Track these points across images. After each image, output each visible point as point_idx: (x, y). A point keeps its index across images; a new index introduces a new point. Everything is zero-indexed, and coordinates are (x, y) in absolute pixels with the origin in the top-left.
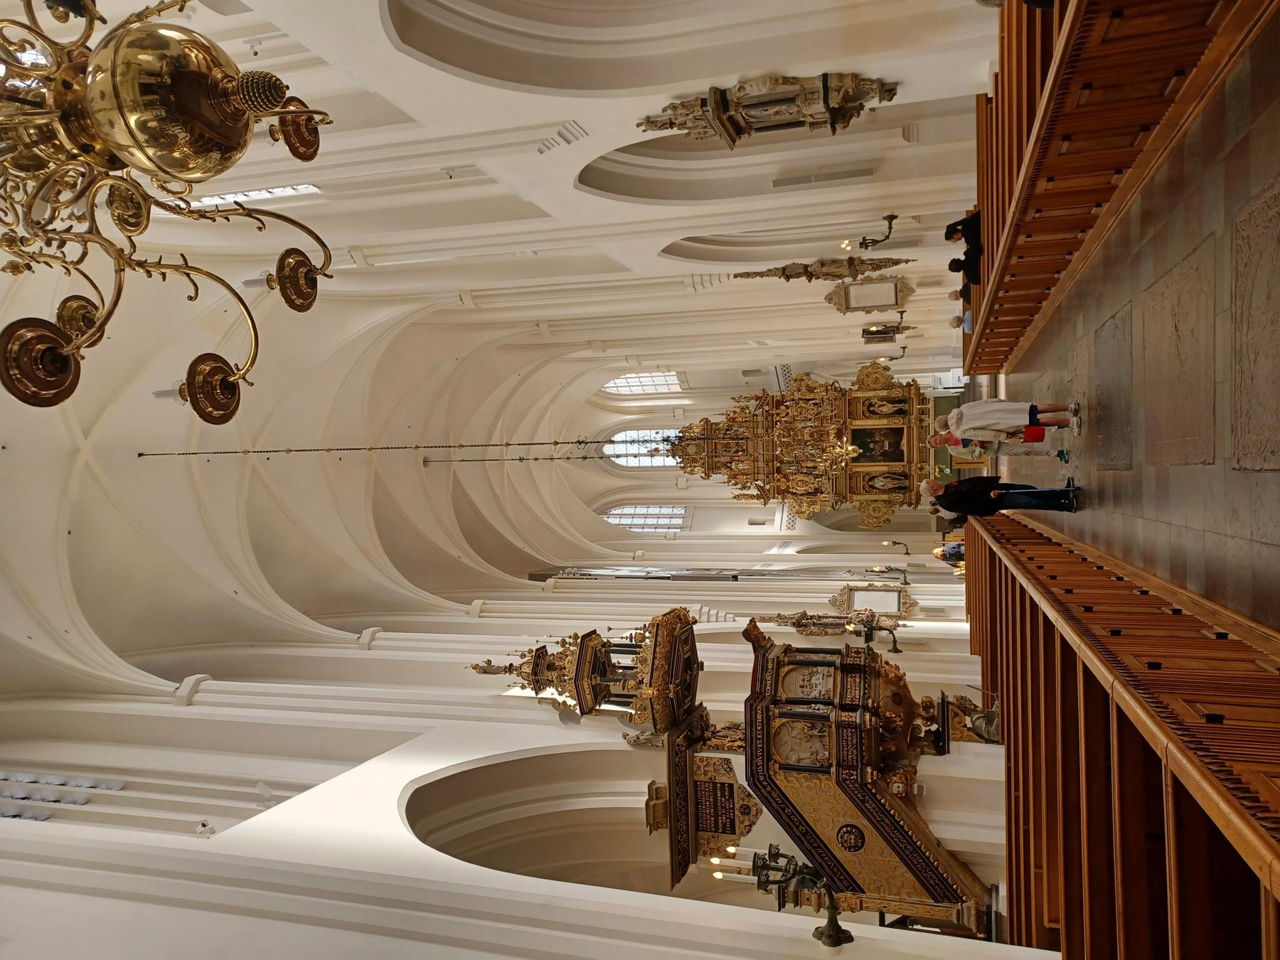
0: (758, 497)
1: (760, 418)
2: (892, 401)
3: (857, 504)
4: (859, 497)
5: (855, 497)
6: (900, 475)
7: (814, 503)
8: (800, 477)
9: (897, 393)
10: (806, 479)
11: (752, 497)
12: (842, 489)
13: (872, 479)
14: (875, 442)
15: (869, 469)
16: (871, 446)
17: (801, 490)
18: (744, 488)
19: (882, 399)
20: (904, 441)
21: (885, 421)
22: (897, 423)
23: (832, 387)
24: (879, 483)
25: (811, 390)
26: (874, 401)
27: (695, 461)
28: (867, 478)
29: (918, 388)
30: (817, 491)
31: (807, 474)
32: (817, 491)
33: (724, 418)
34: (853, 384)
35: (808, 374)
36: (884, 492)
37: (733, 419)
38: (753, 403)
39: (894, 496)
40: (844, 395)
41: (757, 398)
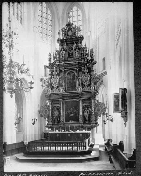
0: (50, 64)
1: (83, 61)
2: (90, 116)
6: (59, 121)
7: (48, 87)
8: (58, 80)
9: (93, 118)
10: (57, 83)
12: (53, 97)
14: (73, 111)
15: (62, 108)
16: (71, 109)
17: (53, 80)
18: (54, 58)
19: (90, 112)
20: (73, 122)
21: (81, 114)
22: (81, 119)
24: (56, 112)
25: (95, 84)
26: (89, 109)
27: (65, 35)
28: (59, 108)
29: (94, 127)
30: (52, 88)
31: (59, 83)
32: (52, 88)
33: (84, 46)
34: (97, 101)
35: (102, 81)
36: (52, 114)
40: (92, 97)
41: (92, 60)
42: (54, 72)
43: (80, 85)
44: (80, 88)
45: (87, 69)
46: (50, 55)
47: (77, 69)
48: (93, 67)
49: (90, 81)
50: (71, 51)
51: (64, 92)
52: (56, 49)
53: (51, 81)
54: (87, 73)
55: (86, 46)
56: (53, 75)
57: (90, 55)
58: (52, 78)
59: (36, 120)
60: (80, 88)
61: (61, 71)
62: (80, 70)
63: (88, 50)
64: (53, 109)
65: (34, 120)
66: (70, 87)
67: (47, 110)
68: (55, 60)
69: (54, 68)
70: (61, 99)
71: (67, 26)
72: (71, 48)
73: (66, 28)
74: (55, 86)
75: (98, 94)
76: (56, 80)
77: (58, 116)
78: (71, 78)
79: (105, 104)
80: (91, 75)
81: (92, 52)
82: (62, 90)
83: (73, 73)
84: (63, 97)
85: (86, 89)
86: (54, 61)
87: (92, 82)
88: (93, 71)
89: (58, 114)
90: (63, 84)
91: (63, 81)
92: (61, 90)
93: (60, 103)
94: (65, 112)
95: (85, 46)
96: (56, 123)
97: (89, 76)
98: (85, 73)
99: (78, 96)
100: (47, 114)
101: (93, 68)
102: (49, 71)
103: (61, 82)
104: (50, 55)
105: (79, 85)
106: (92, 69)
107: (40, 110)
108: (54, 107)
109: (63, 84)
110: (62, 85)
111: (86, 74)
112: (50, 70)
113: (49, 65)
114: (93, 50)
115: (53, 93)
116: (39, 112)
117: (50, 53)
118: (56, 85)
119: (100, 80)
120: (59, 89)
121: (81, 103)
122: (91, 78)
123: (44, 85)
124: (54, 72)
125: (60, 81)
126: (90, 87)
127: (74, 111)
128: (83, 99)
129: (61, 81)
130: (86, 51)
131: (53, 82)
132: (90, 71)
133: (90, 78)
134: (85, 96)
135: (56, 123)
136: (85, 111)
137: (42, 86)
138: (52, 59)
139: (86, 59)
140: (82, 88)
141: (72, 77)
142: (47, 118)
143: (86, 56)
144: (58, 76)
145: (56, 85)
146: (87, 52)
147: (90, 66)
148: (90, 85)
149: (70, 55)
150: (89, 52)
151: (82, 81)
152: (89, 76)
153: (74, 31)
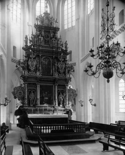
0: (26, 46)
3: (23, 86)
4: (26, 86)
5: (26, 85)
7: (24, 69)
8: (35, 63)
11: (26, 43)
13: (33, 92)
16: (46, 93)
17: (30, 63)
18: (30, 41)
23: (70, 79)
30: (29, 70)
31: (36, 66)
32: (29, 70)
33: (59, 37)
35: (74, 71)
36: (28, 97)
37: (58, 40)
38: (64, 49)
39: (26, 102)
42: (32, 55)
43: (56, 71)
44: (56, 75)
45: (63, 58)
46: (26, 37)
47: (54, 57)
48: (66, 57)
49: (65, 69)
50: (47, 38)
51: (41, 76)
52: (33, 33)
53: (27, 64)
54: (63, 61)
55: (61, 38)
56: (31, 58)
57: (64, 45)
58: (29, 61)
59: (83, 102)
60: (56, 74)
61: (38, 56)
62: (56, 58)
63: (62, 41)
64: (30, 93)
65: (80, 102)
66: (46, 72)
67: (22, 92)
68: (32, 43)
69: (31, 51)
70: (37, 82)
71: (44, 15)
72: (48, 35)
73: (44, 16)
74: (32, 69)
75: (71, 81)
76: (33, 64)
77: (34, 98)
78: (47, 63)
79: (75, 91)
80: (65, 64)
81: (66, 44)
82: (39, 73)
83: (49, 59)
84: (40, 80)
85: (62, 76)
86: (30, 44)
87: (67, 71)
88: (67, 60)
89: (34, 97)
90: (40, 68)
91: (40, 65)
92: (38, 73)
93: (37, 86)
94: (40, 96)
95: (60, 37)
96: (31, 106)
97: (64, 64)
98: (61, 61)
99: (54, 81)
100: (22, 95)
101: (66, 58)
102: (25, 53)
103: (38, 66)
104: (26, 37)
105: (55, 72)
106: (66, 59)
107: (14, 91)
108: (29, 89)
109: (40, 68)
110: (39, 68)
111: (61, 62)
112: (26, 53)
113: (25, 47)
114: (67, 42)
115: (30, 75)
116: (13, 93)
117: (26, 36)
118: (33, 68)
119: (72, 69)
120: (36, 73)
121: (56, 88)
122: (66, 66)
123: (19, 66)
124: (32, 55)
125: (37, 64)
126: (65, 74)
127: (49, 95)
128: (59, 85)
129: (38, 65)
130: (61, 42)
131: (30, 64)
132: (65, 61)
133: (65, 67)
134: (62, 83)
135: (31, 106)
136: (60, 96)
137: (17, 66)
138: (28, 41)
139: (62, 49)
140: (58, 74)
141: (47, 63)
142: (21, 99)
143: (60, 46)
144: (35, 60)
145: (33, 68)
146: (62, 43)
147: (64, 56)
148: (64, 73)
149: (46, 42)
150: (64, 43)
151: (58, 68)
152: (64, 65)
153: (51, 21)
